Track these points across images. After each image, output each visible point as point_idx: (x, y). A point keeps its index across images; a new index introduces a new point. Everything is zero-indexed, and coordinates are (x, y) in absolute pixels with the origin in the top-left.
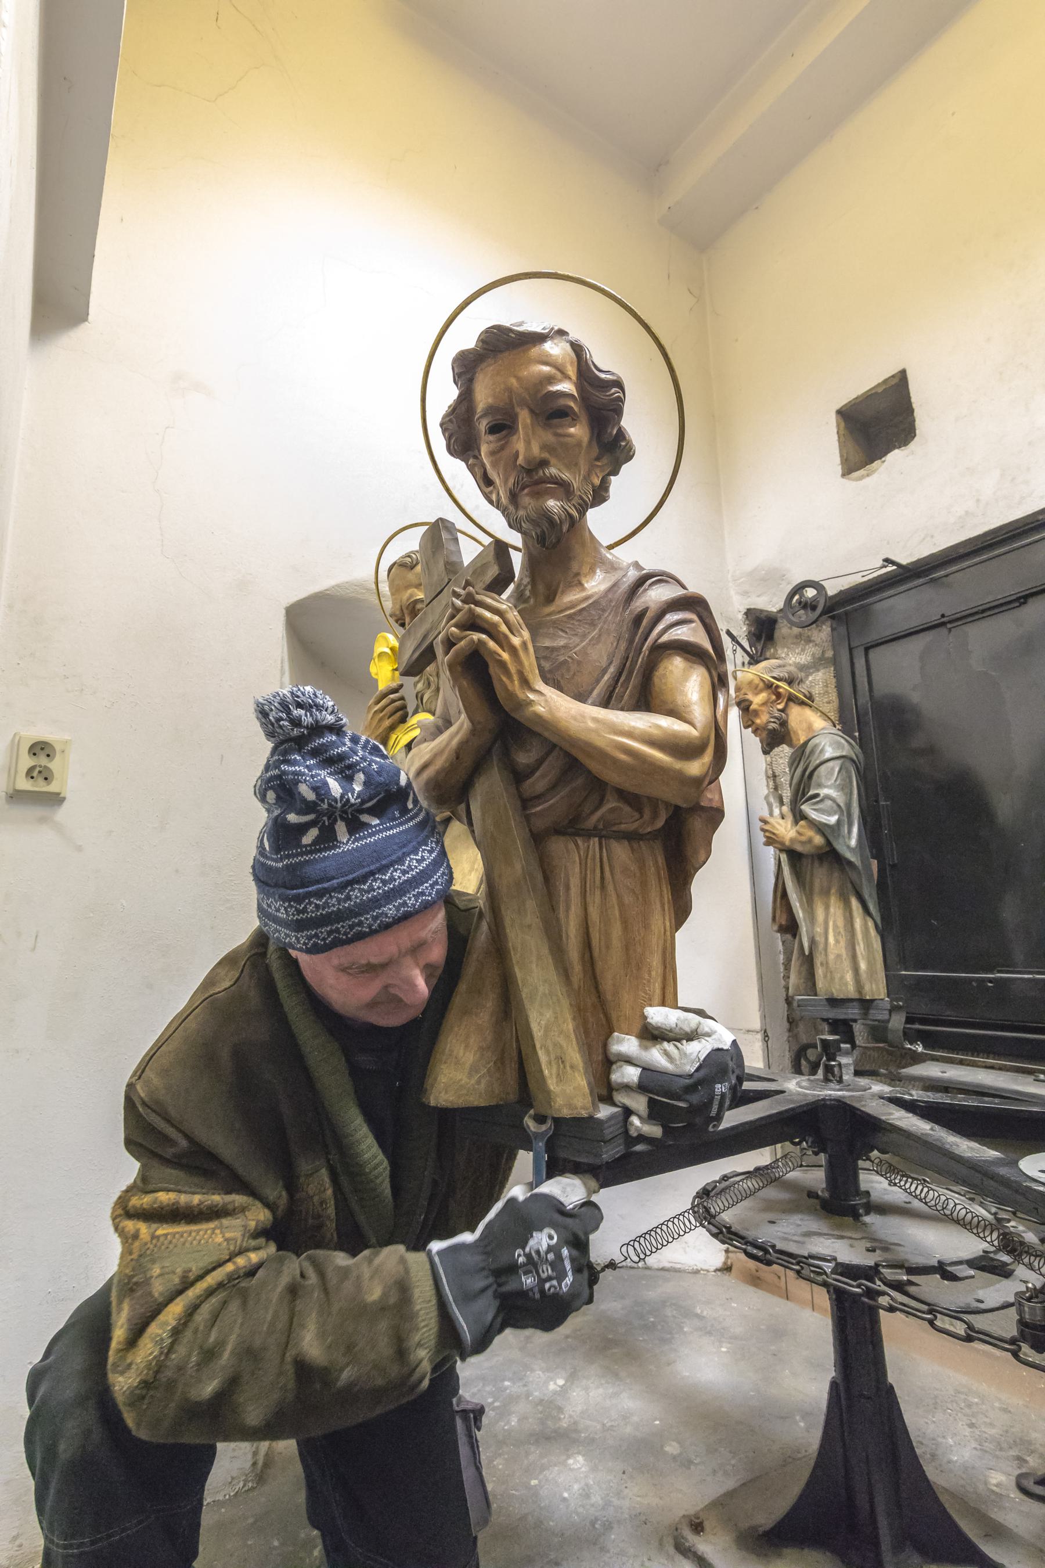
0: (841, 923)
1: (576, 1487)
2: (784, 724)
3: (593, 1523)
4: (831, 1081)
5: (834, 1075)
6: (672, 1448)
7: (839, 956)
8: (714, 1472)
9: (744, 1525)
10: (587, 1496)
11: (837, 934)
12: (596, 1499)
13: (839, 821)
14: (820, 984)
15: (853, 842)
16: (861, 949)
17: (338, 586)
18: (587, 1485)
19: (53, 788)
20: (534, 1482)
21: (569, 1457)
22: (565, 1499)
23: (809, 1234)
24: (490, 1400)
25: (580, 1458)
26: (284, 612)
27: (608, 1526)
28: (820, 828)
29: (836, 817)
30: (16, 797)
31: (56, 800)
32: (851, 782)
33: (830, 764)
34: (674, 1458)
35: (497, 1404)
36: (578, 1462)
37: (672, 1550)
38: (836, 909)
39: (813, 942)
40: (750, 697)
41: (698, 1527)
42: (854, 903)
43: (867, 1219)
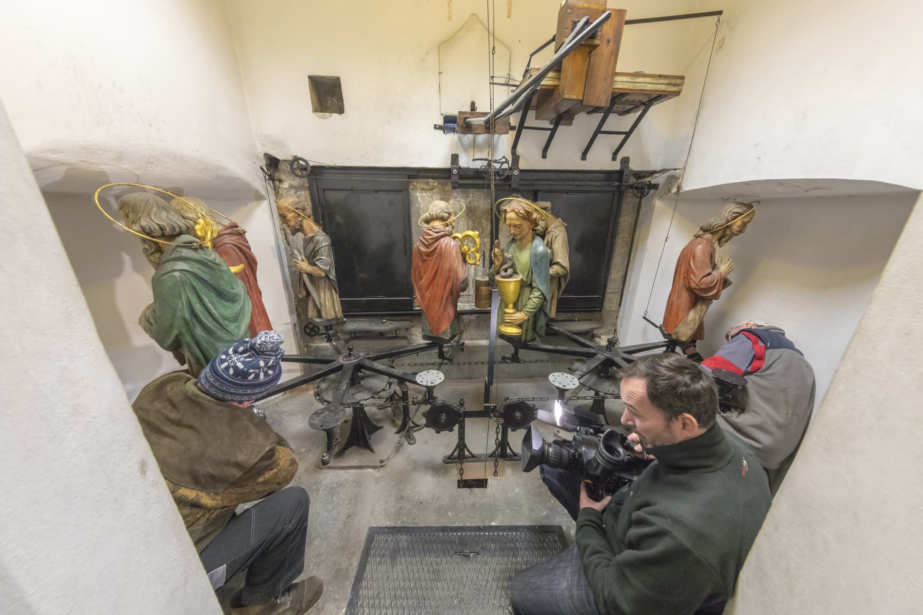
2: (301, 226)
6: (303, 450)
14: (324, 315)
16: (336, 305)
23: (353, 394)
28: (324, 271)
38: (328, 293)
39: (321, 304)
40: (286, 213)
43: (362, 382)
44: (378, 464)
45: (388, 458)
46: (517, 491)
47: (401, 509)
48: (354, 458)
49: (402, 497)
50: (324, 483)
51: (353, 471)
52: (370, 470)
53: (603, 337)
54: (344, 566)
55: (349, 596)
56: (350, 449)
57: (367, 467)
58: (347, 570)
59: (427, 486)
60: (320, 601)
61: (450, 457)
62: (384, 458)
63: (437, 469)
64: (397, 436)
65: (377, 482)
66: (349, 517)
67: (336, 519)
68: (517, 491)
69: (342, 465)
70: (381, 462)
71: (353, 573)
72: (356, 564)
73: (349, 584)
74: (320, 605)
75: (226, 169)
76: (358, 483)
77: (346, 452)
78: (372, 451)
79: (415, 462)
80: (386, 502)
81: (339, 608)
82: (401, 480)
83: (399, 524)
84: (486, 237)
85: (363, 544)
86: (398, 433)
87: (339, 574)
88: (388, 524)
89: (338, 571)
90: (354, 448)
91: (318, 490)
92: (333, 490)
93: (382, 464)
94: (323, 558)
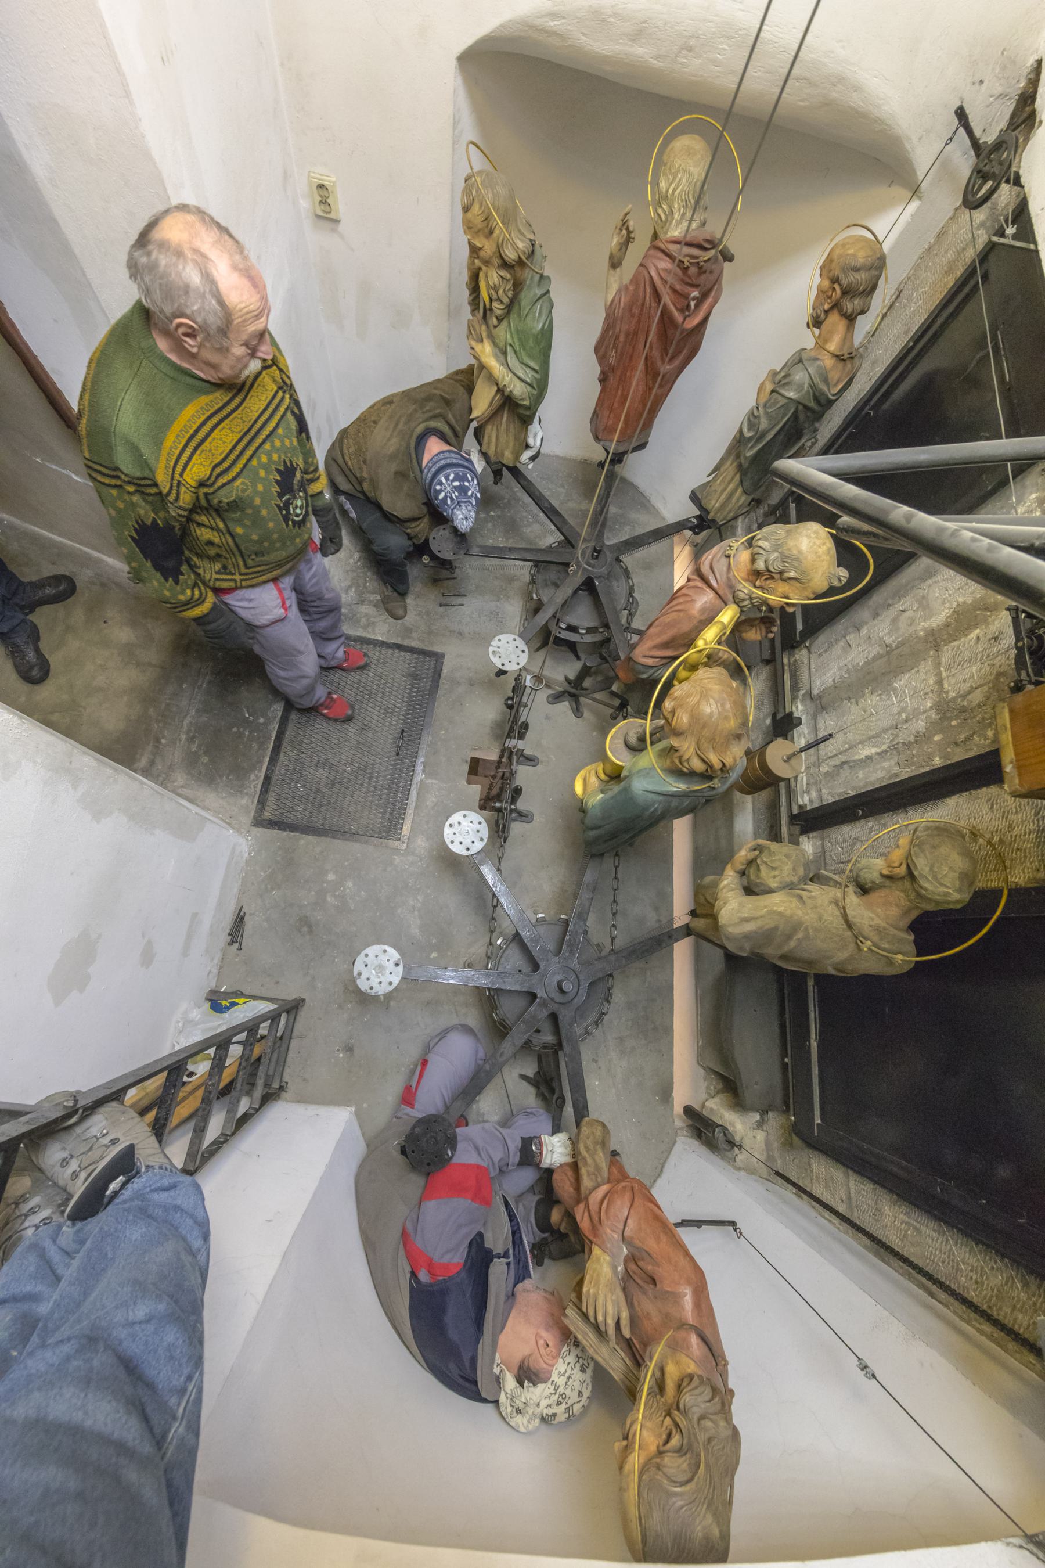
0: (729, 478)
7: (716, 491)
11: (723, 480)
13: (750, 439)
15: (749, 454)
17: (502, 26)
19: (332, 216)
26: (454, 62)
27: (517, 580)
29: (751, 434)
30: (318, 216)
31: (337, 221)
32: (783, 418)
33: (780, 398)
42: (738, 477)
53: (760, 1136)
54: (414, 634)
58: (410, 638)
60: (391, 620)
64: (562, 678)
66: (460, 634)
67: (460, 622)
71: (406, 643)
72: (414, 644)
73: (399, 641)
75: (857, 88)
80: (469, 669)
84: (944, 757)
85: (430, 649)
86: (567, 679)
87: (408, 631)
88: (445, 671)
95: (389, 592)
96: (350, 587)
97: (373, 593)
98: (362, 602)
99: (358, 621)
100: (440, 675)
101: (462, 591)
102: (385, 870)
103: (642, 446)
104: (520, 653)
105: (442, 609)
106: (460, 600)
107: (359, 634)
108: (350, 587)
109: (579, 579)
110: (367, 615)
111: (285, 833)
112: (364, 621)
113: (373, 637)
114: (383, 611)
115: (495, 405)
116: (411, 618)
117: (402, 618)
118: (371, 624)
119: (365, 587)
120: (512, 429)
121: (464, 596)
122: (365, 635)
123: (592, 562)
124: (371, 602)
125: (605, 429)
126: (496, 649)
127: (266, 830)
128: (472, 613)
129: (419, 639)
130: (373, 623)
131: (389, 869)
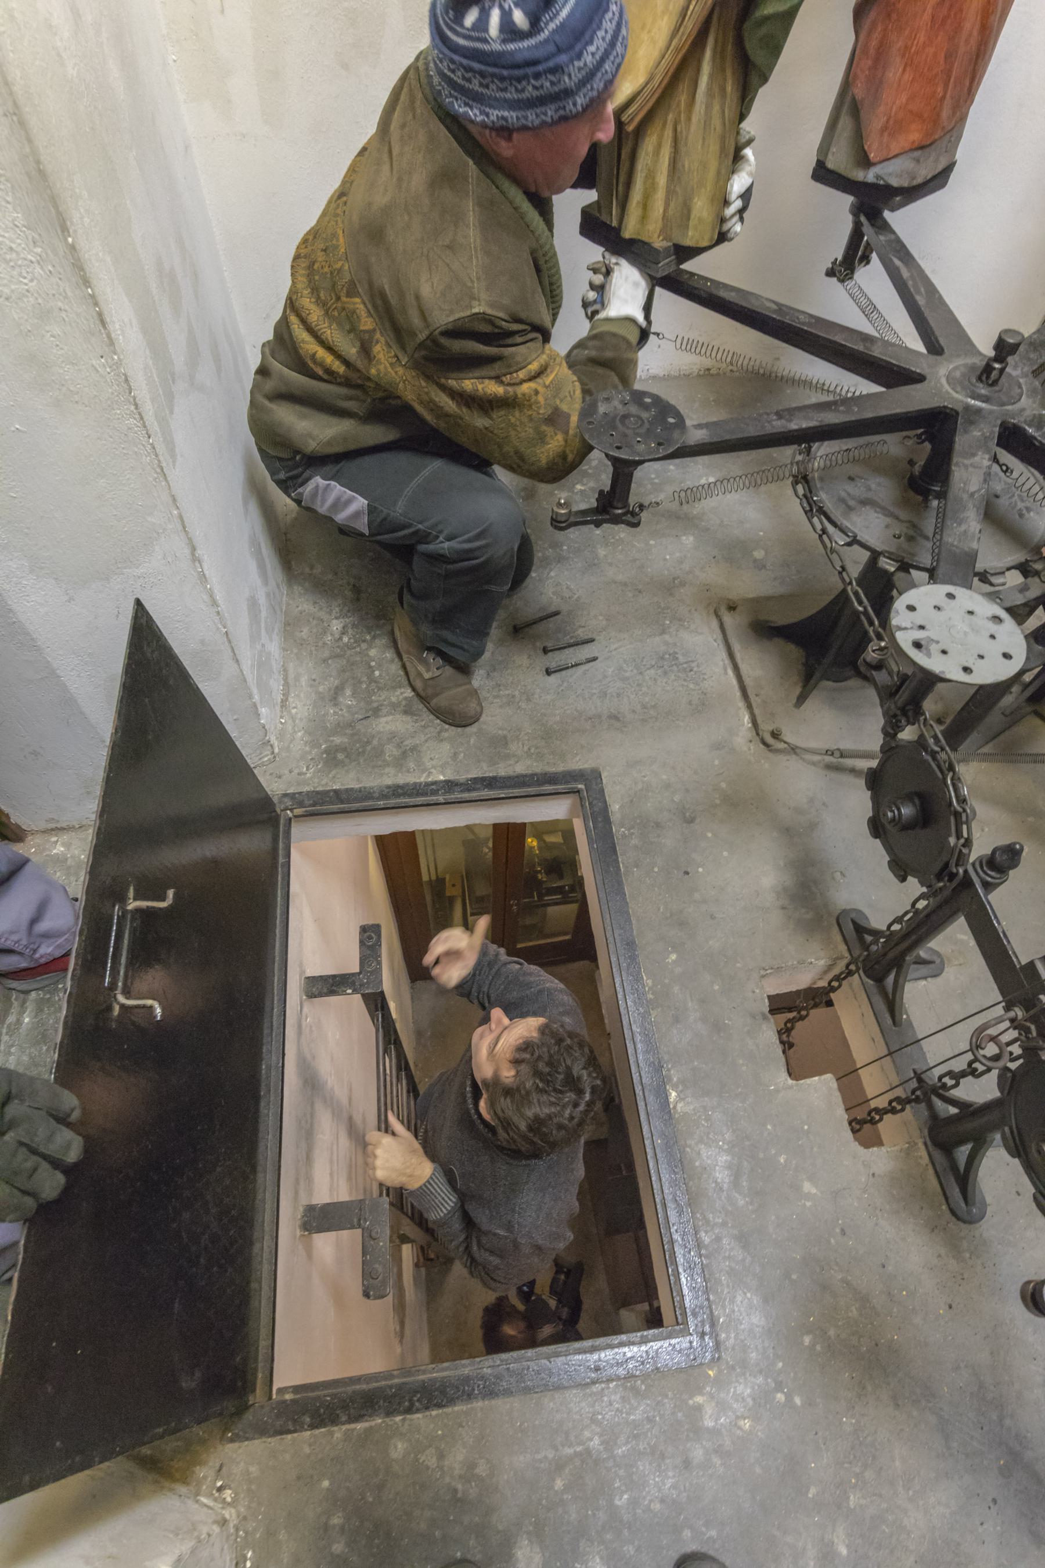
1: (678, 555)
3: (674, 579)
4: (981, 381)
5: (988, 378)
8: (775, 579)
9: (763, 617)
10: (682, 563)
12: (686, 567)
18: (685, 556)
20: (652, 542)
21: (684, 535)
22: (665, 560)
24: (653, 476)
25: (691, 538)
27: (683, 584)
34: (755, 561)
35: (656, 481)
36: (688, 540)
37: (712, 611)
41: (732, 608)
44: (766, 727)
45: (794, 750)
46: (808, 1187)
47: (658, 825)
48: (760, 665)
49: (691, 821)
50: (684, 635)
51: (734, 682)
52: (746, 718)
54: (514, 747)
55: (463, 777)
56: (791, 647)
57: (750, 707)
58: (507, 757)
59: (746, 877)
60: (452, 731)
61: (860, 930)
62: (789, 736)
63: (807, 894)
65: (717, 746)
66: (614, 717)
67: (604, 694)
68: (808, 1187)
69: (737, 647)
70: (775, 735)
74: (446, 735)
76: (701, 706)
77: (779, 642)
78: (801, 700)
79: (812, 826)
80: (668, 786)
81: (443, 767)
82: (739, 804)
83: (618, 831)
85: (561, 768)
87: (499, 743)
88: (615, 807)
89: (504, 741)
90: (794, 651)
91: (663, 632)
92: (670, 661)
93: (770, 740)
94: (523, 705)
95: (431, 669)
96: (338, 690)
97: (394, 688)
98: (376, 712)
99: (379, 753)
100: (607, 821)
101: (581, 634)
102: (687, 1464)
103: (939, 179)
104: (993, 628)
105: (553, 679)
106: (585, 652)
107: (388, 781)
108: (338, 690)
109: (988, 430)
110: (393, 735)
111: (338, 1432)
112: (391, 751)
113: (423, 779)
114: (427, 717)
115: (691, 26)
116: (494, 718)
117: (475, 719)
118: (407, 754)
119: (372, 680)
120: (716, 122)
121: (592, 640)
122: (401, 779)
123: (983, 391)
124: (394, 706)
125: (884, 129)
126: (919, 635)
127: (273, 1442)
128: (621, 669)
129: (529, 754)
130: (414, 749)
131: (698, 1453)
